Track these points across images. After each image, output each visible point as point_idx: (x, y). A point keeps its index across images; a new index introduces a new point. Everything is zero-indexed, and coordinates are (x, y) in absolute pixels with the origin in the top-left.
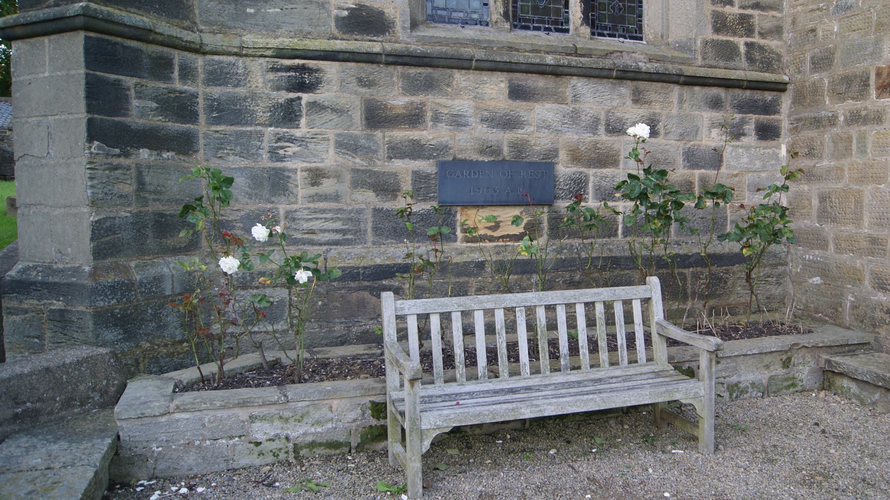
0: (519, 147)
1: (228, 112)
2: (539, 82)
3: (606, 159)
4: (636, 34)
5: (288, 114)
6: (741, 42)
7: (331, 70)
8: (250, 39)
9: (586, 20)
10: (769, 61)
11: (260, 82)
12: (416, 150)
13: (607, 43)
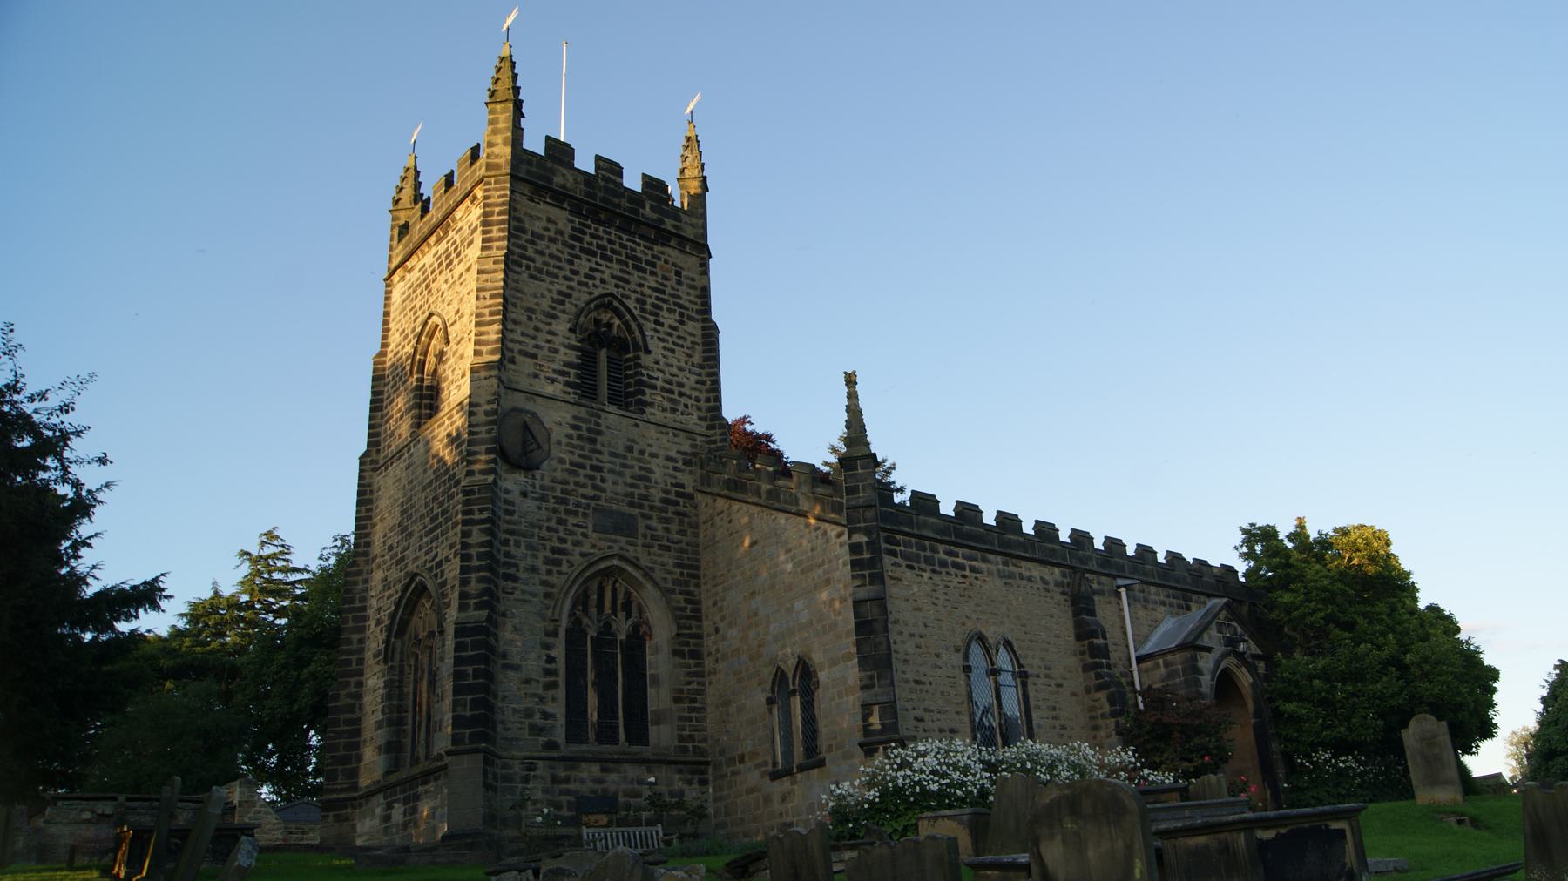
0: (605, 790)
1: (508, 779)
2: (611, 766)
3: (638, 795)
4: (647, 744)
5: (526, 780)
6: (690, 745)
7: (540, 763)
8: (515, 753)
9: (628, 739)
10: (702, 752)
11: (517, 767)
13: (635, 748)
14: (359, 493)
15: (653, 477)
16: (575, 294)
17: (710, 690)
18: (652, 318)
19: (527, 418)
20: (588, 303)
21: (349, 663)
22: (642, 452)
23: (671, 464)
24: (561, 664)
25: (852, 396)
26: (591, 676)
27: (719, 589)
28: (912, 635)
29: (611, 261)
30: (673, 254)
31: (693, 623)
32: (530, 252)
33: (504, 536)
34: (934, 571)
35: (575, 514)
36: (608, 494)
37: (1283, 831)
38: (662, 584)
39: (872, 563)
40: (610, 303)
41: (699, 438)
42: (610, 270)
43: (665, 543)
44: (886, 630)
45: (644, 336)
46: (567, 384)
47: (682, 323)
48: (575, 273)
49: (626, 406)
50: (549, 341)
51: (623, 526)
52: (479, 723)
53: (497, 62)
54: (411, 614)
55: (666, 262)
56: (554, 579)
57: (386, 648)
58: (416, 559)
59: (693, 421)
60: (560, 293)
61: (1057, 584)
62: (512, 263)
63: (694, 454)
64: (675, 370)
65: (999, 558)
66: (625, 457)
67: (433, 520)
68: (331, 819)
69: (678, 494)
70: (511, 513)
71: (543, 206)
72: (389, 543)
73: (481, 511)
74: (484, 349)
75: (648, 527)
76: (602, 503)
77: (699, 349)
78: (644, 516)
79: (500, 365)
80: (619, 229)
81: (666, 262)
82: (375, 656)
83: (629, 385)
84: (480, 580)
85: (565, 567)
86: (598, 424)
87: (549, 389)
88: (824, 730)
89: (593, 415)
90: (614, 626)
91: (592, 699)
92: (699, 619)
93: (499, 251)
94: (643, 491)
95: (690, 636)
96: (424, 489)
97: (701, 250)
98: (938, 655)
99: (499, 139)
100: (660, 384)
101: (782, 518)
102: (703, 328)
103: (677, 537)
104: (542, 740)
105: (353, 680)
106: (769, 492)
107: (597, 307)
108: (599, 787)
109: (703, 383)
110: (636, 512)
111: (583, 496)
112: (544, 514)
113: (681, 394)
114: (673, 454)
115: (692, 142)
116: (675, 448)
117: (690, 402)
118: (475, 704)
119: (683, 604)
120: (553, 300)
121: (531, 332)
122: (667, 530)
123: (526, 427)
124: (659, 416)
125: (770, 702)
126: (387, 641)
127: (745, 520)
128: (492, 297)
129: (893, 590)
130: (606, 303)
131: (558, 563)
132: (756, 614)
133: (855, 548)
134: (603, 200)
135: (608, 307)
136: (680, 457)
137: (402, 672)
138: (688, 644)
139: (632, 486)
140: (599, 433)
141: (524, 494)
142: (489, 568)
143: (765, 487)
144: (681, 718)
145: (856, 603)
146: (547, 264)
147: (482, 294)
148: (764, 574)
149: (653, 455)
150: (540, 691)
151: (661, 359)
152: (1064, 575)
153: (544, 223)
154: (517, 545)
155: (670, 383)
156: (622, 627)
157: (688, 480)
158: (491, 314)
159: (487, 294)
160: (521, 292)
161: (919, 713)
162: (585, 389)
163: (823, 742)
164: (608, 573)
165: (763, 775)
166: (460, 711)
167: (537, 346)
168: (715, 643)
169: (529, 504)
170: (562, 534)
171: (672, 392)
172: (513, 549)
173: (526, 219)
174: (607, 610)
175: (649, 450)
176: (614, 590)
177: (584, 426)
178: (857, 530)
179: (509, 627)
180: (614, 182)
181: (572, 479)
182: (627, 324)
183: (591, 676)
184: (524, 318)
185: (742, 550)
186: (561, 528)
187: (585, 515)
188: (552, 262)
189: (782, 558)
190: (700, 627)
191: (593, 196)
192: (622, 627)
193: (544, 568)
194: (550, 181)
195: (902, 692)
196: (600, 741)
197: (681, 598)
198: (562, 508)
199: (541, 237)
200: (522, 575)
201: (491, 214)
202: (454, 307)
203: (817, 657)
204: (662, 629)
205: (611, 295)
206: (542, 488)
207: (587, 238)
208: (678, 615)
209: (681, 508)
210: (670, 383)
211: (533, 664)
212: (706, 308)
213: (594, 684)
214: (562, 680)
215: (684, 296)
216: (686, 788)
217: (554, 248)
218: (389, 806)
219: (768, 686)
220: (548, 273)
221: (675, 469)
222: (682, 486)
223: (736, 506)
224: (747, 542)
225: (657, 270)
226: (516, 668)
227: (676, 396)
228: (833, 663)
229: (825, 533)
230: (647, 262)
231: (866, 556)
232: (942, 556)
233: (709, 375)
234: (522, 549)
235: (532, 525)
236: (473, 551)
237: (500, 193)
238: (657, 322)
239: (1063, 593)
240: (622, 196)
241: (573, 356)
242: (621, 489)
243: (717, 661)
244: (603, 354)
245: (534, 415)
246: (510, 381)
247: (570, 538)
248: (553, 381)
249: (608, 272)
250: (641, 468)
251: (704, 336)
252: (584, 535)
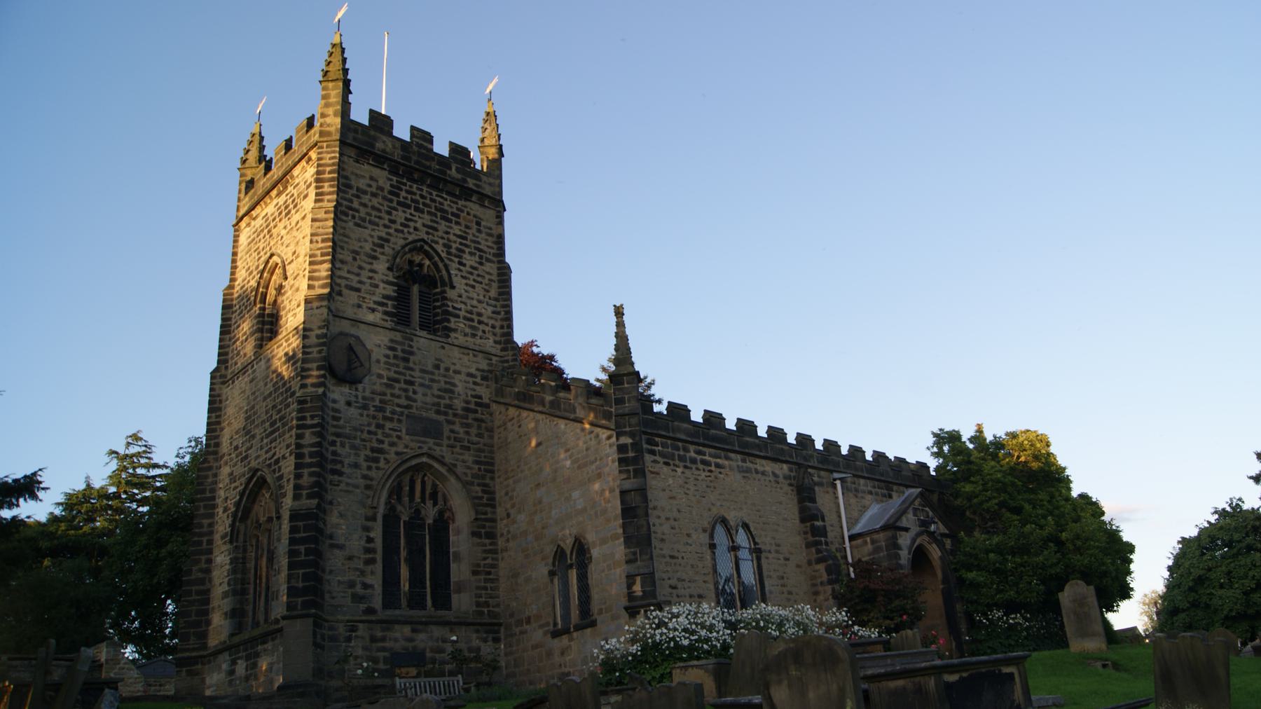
1: (333, 639)
2: (420, 627)
3: (442, 651)
4: (449, 609)
5: (349, 639)
7: (361, 626)
8: (340, 617)
9: (434, 605)
11: (342, 630)
12: (383, 649)
13: (440, 613)
14: (210, 403)
15: (456, 390)
16: (393, 239)
17: (502, 565)
18: (456, 260)
19: (352, 341)
20: (403, 247)
21: (200, 543)
22: (447, 369)
23: (471, 380)
24: (379, 544)
25: (620, 325)
26: (403, 554)
27: (511, 481)
28: (668, 519)
29: (422, 212)
30: (474, 208)
31: (489, 509)
32: (356, 205)
33: (331, 438)
34: (686, 467)
35: (391, 420)
36: (419, 404)
37: (965, 675)
38: (464, 478)
39: (637, 460)
40: (422, 247)
41: (494, 358)
42: (422, 220)
43: (466, 444)
44: (647, 515)
45: (449, 275)
46: (386, 313)
47: (481, 264)
48: (393, 222)
49: (435, 332)
50: (371, 278)
51: (431, 430)
52: (310, 592)
53: (329, 48)
54: (254, 502)
55: (468, 214)
56: (373, 474)
57: (232, 531)
58: (258, 457)
59: (489, 344)
60: (380, 238)
61: (786, 477)
62: (340, 213)
63: (490, 371)
64: (475, 303)
65: (739, 457)
66: (433, 374)
67: (272, 424)
68: (184, 674)
69: (477, 404)
70: (338, 419)
71: (366, 167)
72: (235, 444)
73: (312, 417)
74: (316, 283)
75: (452, 431)
76: (414, 410)
77: (495, 285)
78: (449, 422)
79: (329, 297)
80: (429, 186)
81: (468, 214)
82: (223, 538)
83: (437, 315)
84: (311, 474)
85: (382, 464)
86: (411, 346)
87: (371, 317)
88: (596, 595)
89: (406, 338)
90: (423, 512)
91: (404, 572)
92: (494, 507)
93: (329, 203)
94: (447, 402)
95: (486, 520)
96: (265, 399)
97: (497, 204)
98: (688, 535)
99: (330, 111)
100: (462, 313)
101: (562, 424)
102: (499, 269)
103: (475, 439)
104: (363, 606)
105: (203, 558)
106: (552, 403)
107: (410, 251)
108: (410, 645)
109: (498, 313)
110: (442, 418)
111: (399, 406)
112: (365, 420)
113: (480, 322)
114: (473, 371)
115: (491, 117)
116: (475, 366)
117: (487, 329)
118: (306, 577)
119: (480, 494)
120: (374, 244)
121: (356, 270)
122: (467, 433)
123: (350, 348)
124: (461, 340)
125: (552, 574)
126: (232, 526)
127: (532, 425)
128: (323, 241)
129: (653, 482)
130: (418, 247)
131: (376, 460)
132: (540, 502)
133: (622, 449)
134: (417, 162)
135: (420, 250)
136: (478, 374)
137: (245, 551)
138: (484, 527)
139: (439, 397)
140: (412, 353)
141: (349, 404)
142: (319, 465)
143: (549, 398)
144: (478, 588)
145: (623, 493)
146: (370, 215)
147: (315, 238)
148: (548, 470)
149: (458, 372)
150: (361, 566)
151: (464, 292)
152: (791, 470)
153: (368, 181)
154: (343, 445)
155: (471, 312)
156: (430, 513)
157: (485, 393)
158: (322, 255)
159: (319, 239)
160: (348, 237)
161: (673, 582)
162: (400, 317)
163: (595, 606)
164: (418, 468)
165: (545, 634)
166: (294, 583)
167: (360, 282)
168: (506, 526)
169: (353, 412)
170: (380, 437)
171: (472, 320)
172: (339, 450)
173: (353, 177)
174: (418, 500)
175: (452, 368)
176: (423, 483)
177: (399, 348)
178: (624, 434)
179: (335, 513)
180: (426, 148)
181: (388, 391)
182: (435, 265)
183: (403, 554)
184: (350, 259)
185: (529, 449)
186: (380, 432)
187: (400, 421)
188: (374, 213)
189: (562, 456)
190: (494, 513)
191: (408, 159)
192: (430, 513)
193: (365, 464)
194: (373, 146)
195: (660, 567)
196: (411, 607)
197: (479, 489)
198: (380, 415)
199: (365, 192)
200: (346, 470)
201: (324, 172)
202: (292, 248)
203: (590, 537)
204: (463, 515)
205: (423, 240)
206: (364, 398)
207: (403, 194)
208: (476, 503)
209: (479, 416)
210: (471, 312)
211: (356, 544)
212: (501, 252)
213: (406, 560)
214: (379, 556)
215: (483, 242)
216: (482, 645)
217: (375, 202)
218: (234, 662)
219: (550, 560)
220: (370, 222)
221: (475, 383)
222: (480, 397)
223: (525, 414)
224: (534, 443)
225: (461, 220)
226: (341, 547)
227: (475, 324)
228: (604, 541)
229: (597, 436)
230: (453, 214)
231: (631, 454)
232: (693, 454)
233: (503, 306)
234: (347, 449)
235: (355, 429)
236: (306, 451)
237: (331, 156)
238: (460, 263)
239: (790, 485)
240: (433, 159)
241: (390, 291)
242: (429, 399)
243: (508, 540)
244: (415, 289)
245: (357, 338)
246: (338, 310)
247: (386, 440)
248: (373, 310)
249: (420, 221)
250: (446, 383)
251: (499, 275)
252: (399, 437)
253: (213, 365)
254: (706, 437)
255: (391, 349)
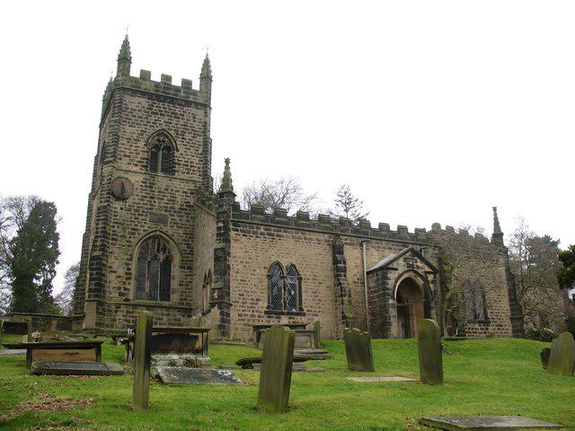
11: (113, 307)
12: (132, 317)
19: (124, 180)
30: (192, 110)
48: (149, 122)
51: (163, 220)
59: (197, 177)
85: (136, 236)
87: (134, 169)
91: (147, 284)
97: (206, 106)
100: (182, 163)
110: (167, 213)
121: (128, 147)
123: (123, 184)
124: (182, 176)
129: (233, 244)
130: (161, 133)
133: (219, 228)
142: (104, 236)
145: (216, 250)
151: (183, 153)
157: (192, 200)
161: (241, 293)
164: (156, 237)
179: (113, 257)
207: (155, 108)
211: (121, 271)
226: (115, 272)
230: (181, 115)
234: (120, 229)
248: (136, 165)
253: (90, 191)
254: (272, 221)
255: (143, 182)
